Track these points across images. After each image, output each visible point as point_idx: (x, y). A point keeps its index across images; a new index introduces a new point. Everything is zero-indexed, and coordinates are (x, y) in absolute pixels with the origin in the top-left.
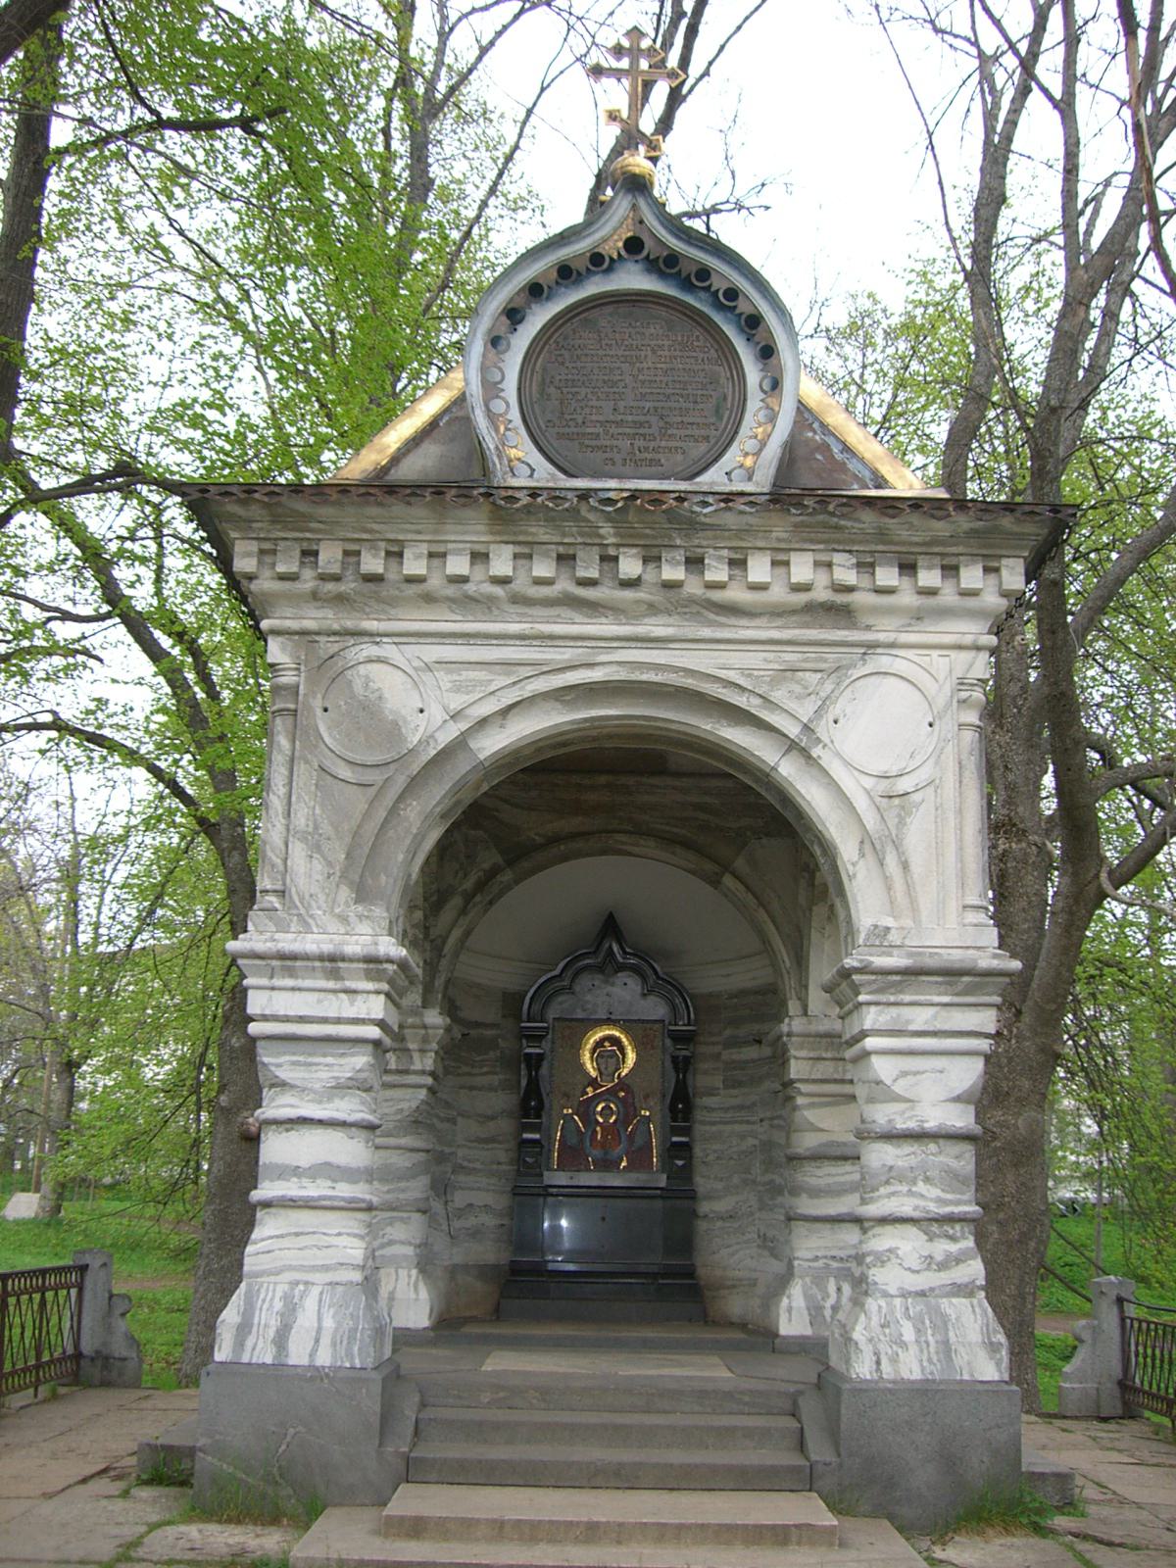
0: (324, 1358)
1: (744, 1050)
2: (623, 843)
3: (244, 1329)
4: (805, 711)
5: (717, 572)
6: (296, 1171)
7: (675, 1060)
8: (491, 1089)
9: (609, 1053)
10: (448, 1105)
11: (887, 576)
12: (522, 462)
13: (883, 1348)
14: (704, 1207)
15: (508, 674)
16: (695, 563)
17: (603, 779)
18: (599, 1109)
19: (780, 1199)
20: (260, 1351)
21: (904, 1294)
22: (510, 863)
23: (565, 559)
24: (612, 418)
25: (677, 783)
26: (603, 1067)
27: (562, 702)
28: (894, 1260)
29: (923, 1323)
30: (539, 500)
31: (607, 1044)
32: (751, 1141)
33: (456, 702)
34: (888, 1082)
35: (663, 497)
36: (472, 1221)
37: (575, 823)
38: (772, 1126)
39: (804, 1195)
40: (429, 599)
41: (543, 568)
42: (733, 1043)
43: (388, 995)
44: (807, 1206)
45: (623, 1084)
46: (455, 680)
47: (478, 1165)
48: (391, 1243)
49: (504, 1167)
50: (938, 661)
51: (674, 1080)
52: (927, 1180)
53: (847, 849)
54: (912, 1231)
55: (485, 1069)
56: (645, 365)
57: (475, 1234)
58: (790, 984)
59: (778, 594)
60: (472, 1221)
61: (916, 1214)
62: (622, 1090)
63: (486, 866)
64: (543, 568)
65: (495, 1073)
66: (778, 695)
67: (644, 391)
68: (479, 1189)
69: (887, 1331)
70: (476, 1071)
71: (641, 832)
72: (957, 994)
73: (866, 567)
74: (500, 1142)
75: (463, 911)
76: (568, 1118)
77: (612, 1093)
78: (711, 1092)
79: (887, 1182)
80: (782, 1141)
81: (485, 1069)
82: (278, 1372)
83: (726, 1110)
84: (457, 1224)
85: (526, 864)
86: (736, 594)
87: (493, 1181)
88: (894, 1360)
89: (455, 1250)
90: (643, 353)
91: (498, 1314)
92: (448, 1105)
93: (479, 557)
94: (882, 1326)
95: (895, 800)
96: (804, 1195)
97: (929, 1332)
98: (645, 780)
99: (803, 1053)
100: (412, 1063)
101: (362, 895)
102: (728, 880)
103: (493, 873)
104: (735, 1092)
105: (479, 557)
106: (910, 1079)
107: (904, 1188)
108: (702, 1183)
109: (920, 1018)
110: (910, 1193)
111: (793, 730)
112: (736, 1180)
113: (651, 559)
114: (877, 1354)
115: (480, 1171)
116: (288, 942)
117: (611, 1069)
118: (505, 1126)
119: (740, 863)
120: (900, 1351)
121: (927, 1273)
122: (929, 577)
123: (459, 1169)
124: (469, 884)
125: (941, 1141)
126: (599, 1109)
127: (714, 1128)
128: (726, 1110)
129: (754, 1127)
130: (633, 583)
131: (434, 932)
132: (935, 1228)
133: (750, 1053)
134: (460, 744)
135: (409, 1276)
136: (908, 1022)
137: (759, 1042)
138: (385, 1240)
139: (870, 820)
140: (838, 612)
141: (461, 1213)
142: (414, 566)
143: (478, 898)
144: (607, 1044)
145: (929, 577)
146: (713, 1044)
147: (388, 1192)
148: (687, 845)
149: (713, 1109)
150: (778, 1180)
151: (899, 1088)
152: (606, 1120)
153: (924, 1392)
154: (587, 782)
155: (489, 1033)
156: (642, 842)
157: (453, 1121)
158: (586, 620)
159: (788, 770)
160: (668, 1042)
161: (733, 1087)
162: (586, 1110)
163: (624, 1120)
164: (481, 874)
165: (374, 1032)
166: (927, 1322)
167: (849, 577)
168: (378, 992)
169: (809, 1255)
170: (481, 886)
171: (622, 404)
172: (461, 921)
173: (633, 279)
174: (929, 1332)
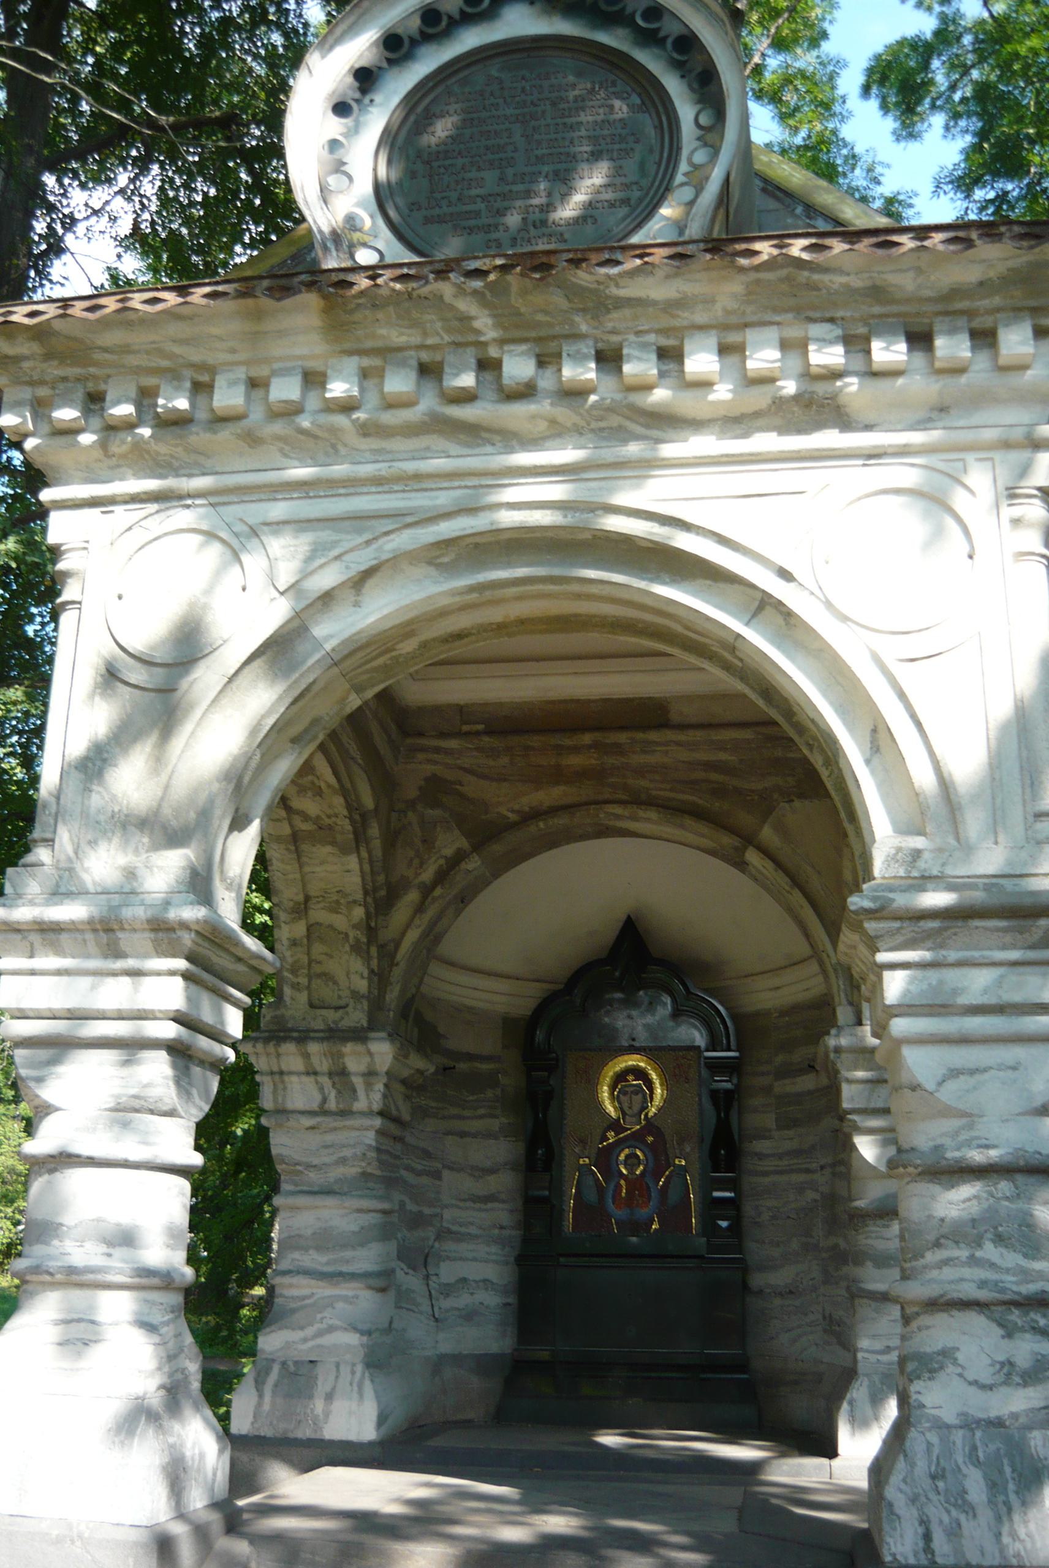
1: (799, 1079)
2: (618, 817)
5: (638, 366)
7: (714, 1094)
8: (489, 1135)
10: (427, 1154)
11: (889, 351)
13: (937, 1513)
14: (757, 1280)
15: (359, 531)
16: (609, 359)
17: (587, 738)
18: (622, 1157)
19: (845, 1269)
21: (969, 1424)
22: (477, 848)
23: (429, 371)
24: (497, 190)
25: (681, 737)
26: (626, 1106)
27: (438, 566)
28: (951, 1369)
29: (1001, 1472)
30: (380, 281)
31: (630, 1078)
32: (811, 1195)
34: (930, 1086)
35: (553, 260)
36: (463, 1300)
37: (555, 794)
38: (834, 1174)
39: (869, 1264)
40: (252, 440)
42: (787, 1072)
43: (187, 976)
45: (651, 1126)
47: (473, 1230)
48: (331, 1329)
49: (506, 1233)
51: (714, 1121)
52: (1000, 1239)
54: (977, 1321)
55: (482, 1111)
56: (542, 122)
57: (470, 1316)
60: (463, 1300)
61: (983, 1295)
62: (650, 1134)
63: (449, 852)
65: (496, 1117)
67: (539, 152)
68: (475, 1259)
69: (941, 1484)
70: (466, 1113)
71: (640, 800)
72: (1032, 947)
73: (857, 343)
74: (504, 1202)
75: (420, 909)
76: (585, 1170)
77: (637, 1138)
78: (763, 1134)
79: (937, 1244)
80: (845, 1193)
81: (482, 1111)
83: (780, 1157)
84: (446, 1303)
85: (497, 848)
87: (494, 1249)
88: (954, 1532)
89: (441, 1336)
90: (539, 109)
91: (501, 1417)
92: (427, 1154)
93: (314, 380)
94: (934, 1477)
96: (869, 1264)
97: (1011, 1486)
98: (640, 736)
99: (860, 1074)
100: (356, 1099)
102: (752, 856)
103: (459, 857)
104: (790, 1133)
106: (963, 1081)
107: (963, 1253)
108: (756, 1249)
110: (973, 1261)
112: (795, 1245)
113: (546, 360)
114: (924, 1522)
115: (477, 1237)
117: (636, 1108)
118: (505, 1182)
119: (767, 834)
120: (963, 1518)
121: (1004, 1390)
122: (951, 346)
123: (443, 1234)
124: (427, 875)
125: (1020, 1179)
126: (622, 1157)
127: (767, 1180)
128: (780, 1157)
129: (815, 1176)
130: (526, 392)
131: (387, 934)
132: (1015, 1316)
133: (806, 1083)
135: (353, 1373)
136: (955, 992)
137: (812, 1067)
138: (324, 1326)
141: (447, 1290)
142: (228, 396)
143: (438, 892)
144: (630, 1078)
145: (951, 346)
146: (763, 1074)
147: (328, 1263)
148: (698, 814)
149: (768, 1156)
150: (842, 1244)
151: (949, 1094)
152: (631, 1171)
154: (567, 742)
155: (485, 1067)
156: (641, 813)
157: (437, 1175)
158: (470, 452)
160: (704, 1072)
161: (788, 1128)
162: (605, 1159)
164: (442, 861)
165: (170, 1030)
166: (1008, 1470)
168: (172, 973)
169: (878, 1345)
170: (441, 877)
171: (510, 172)
172: (417, 921)
174: (1011, 1486)
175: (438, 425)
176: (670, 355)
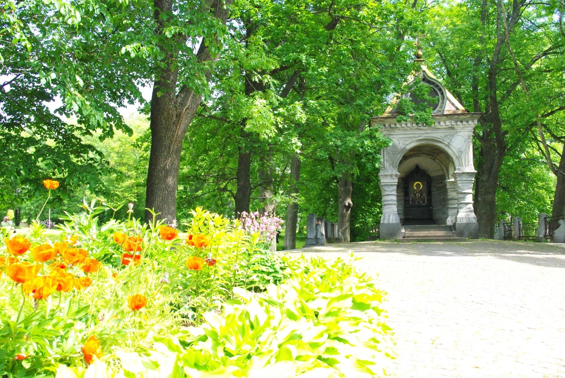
0: (394, 222)
3: (384, 219)
4: (448, 141)
6: (388, 201)
9: (418, 186)
11: (459, 123)
20: (386, 222)
33: (403, 142)
41: (414, 125)
44: (450, 206)
45: (421, 191)
50: (466, 133)
53: (454, 158)
58: (446, 174)
59: (444, 126)
66: (445, 139)
77: (419, 192)
78: (434, 191)
82: (389, 224)
86: (439, 127)
109: (464, 179)
111: (447, 144)
116: (386, 174)
119: (438, 157)
122: (464, 123)
133: (441, 185)
134: (405, 148)
139: (457, 154)
140: (452, 128)
145: (464, 123)
148: (430, 155)
159: (446, 149)
162: (415, 195)
163: (421, 196)
167: (454, 124)
175: (417, 129)
176: (439, 123)
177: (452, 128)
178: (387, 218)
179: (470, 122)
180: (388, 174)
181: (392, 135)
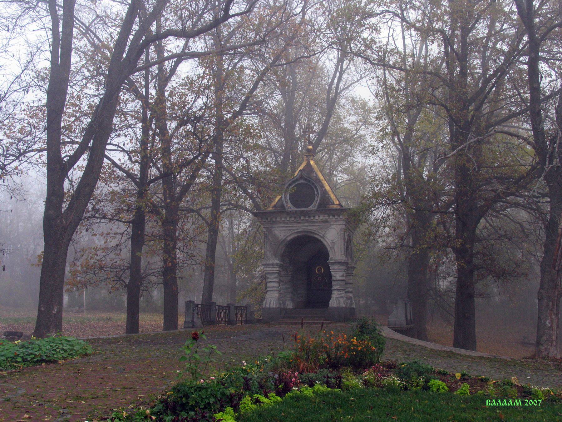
2: (307, 226)
3: (266, 304)
4: (323, 233)
11: (331, 217)
12: (290, 207)
16: (309, 217)
20: (268, 306)
23: (295, 218)
41: (293, 219)
46: (284, 232)
53: (329, 249)
59: (319, 220)
64: (293, 219)
66: (320, 231)
73: (329, 216)
82: (269, 308)
86: (314, 220)
93: (286, 218)
95: (333, 243)
101: (275, 256)
105: (286, 218)
122: (336, 217)
134: (285, 239)
140: (326, 221)
142: (278, 219)
145: (336, 217)
153: (337, 308)
159: (322, 240)
173: (302, 181)
177: (326, 221)
178: (268, 303)
179: (341, 217)
180: (270, 262)
181: (275, 227)
